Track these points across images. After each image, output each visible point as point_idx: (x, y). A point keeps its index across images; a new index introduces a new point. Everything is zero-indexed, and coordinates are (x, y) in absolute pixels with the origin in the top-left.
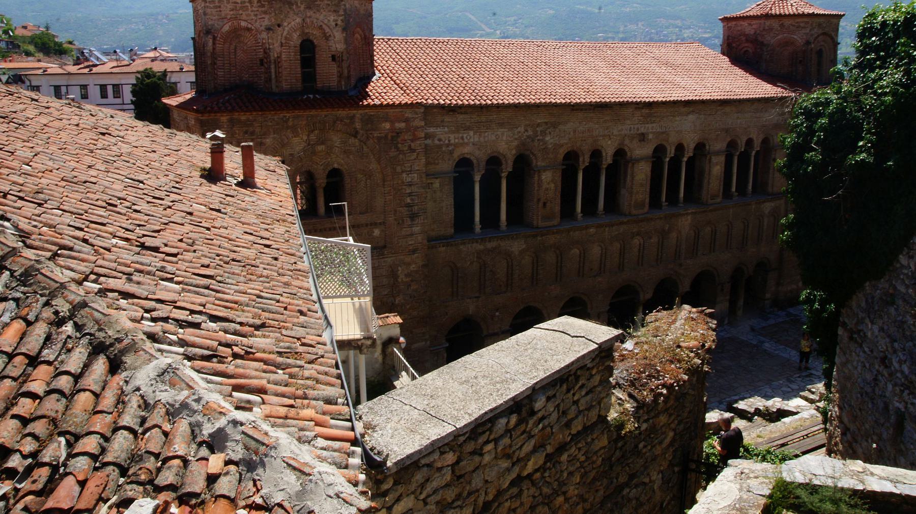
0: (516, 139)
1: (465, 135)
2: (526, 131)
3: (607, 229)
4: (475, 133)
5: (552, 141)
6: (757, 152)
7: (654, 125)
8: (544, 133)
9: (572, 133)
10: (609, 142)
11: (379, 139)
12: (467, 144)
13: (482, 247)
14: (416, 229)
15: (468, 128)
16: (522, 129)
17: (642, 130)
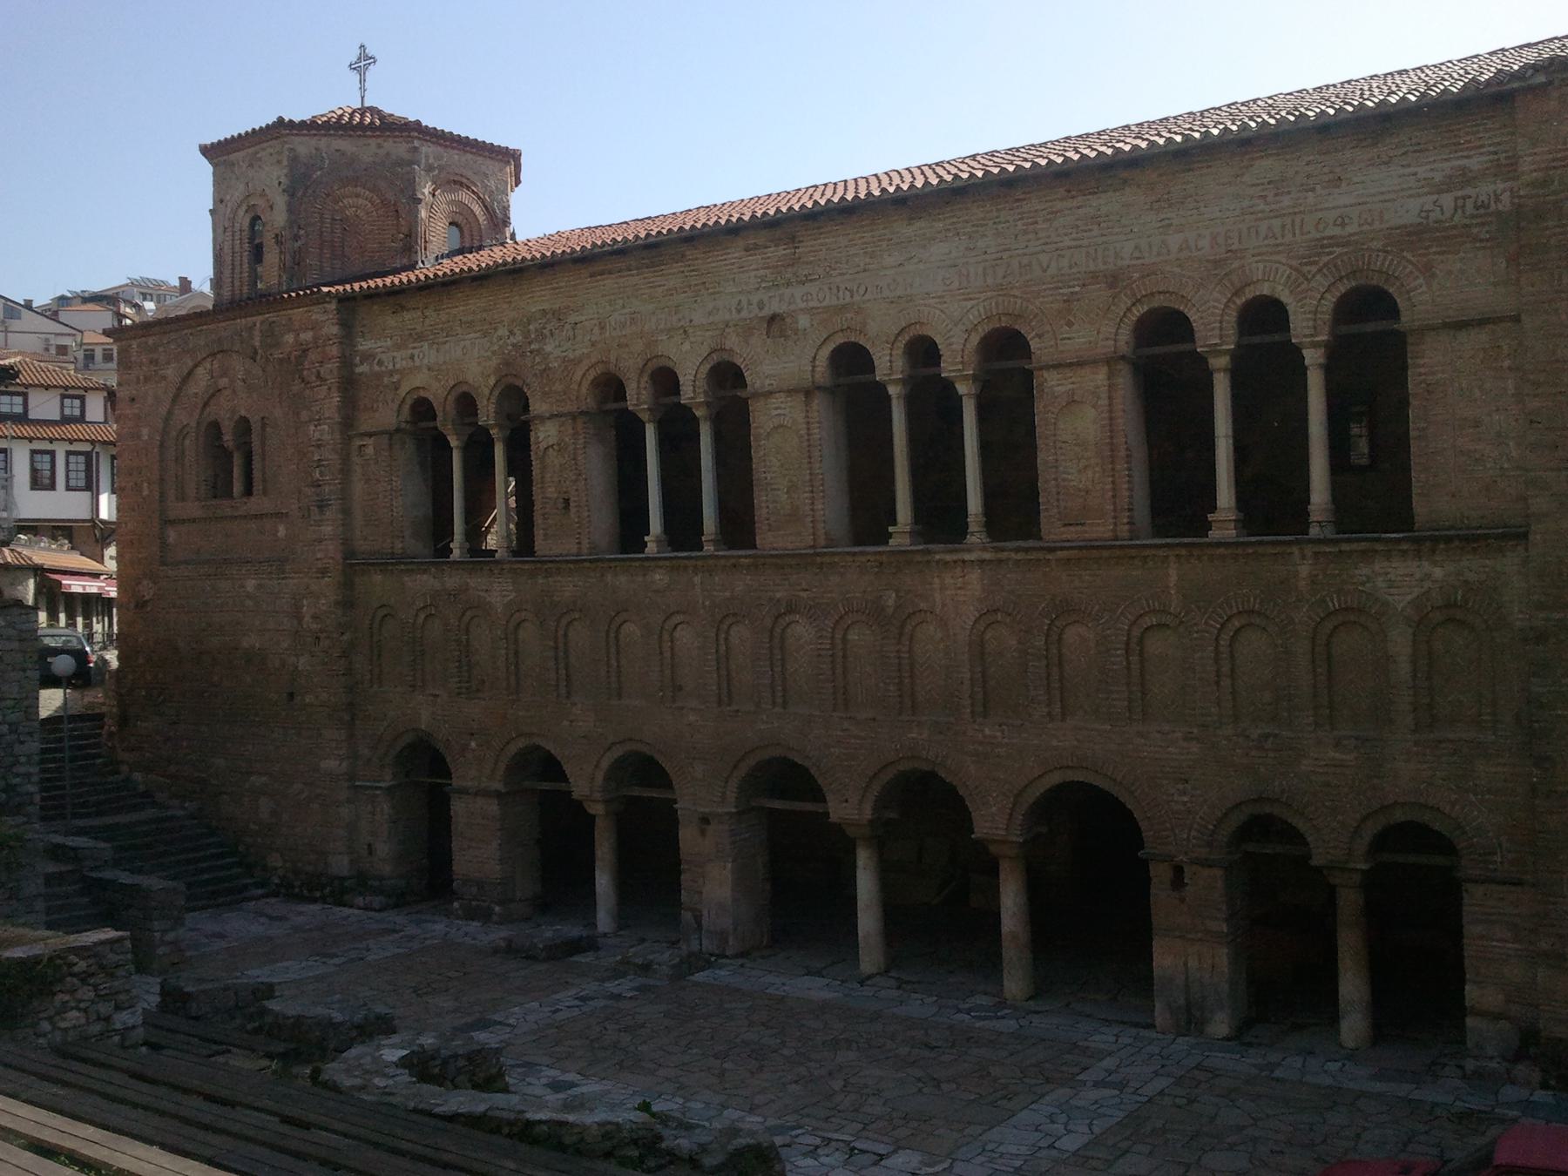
0: (494, 353)
1: (416, 352)
2: (512, 333)
3: (697, 579)
4: (430, 346)
5: (557, 352)
6: (1339, 355)
7: (811, 288)
8: (541, 337)
9: (596, 330)
10: (687, 346)
11: (281, 361)
12: (418, 368)
13: (437, 584)
14: (327, 529)
15: (420, 337)
16: (503, 332)
17: (775, 307)
